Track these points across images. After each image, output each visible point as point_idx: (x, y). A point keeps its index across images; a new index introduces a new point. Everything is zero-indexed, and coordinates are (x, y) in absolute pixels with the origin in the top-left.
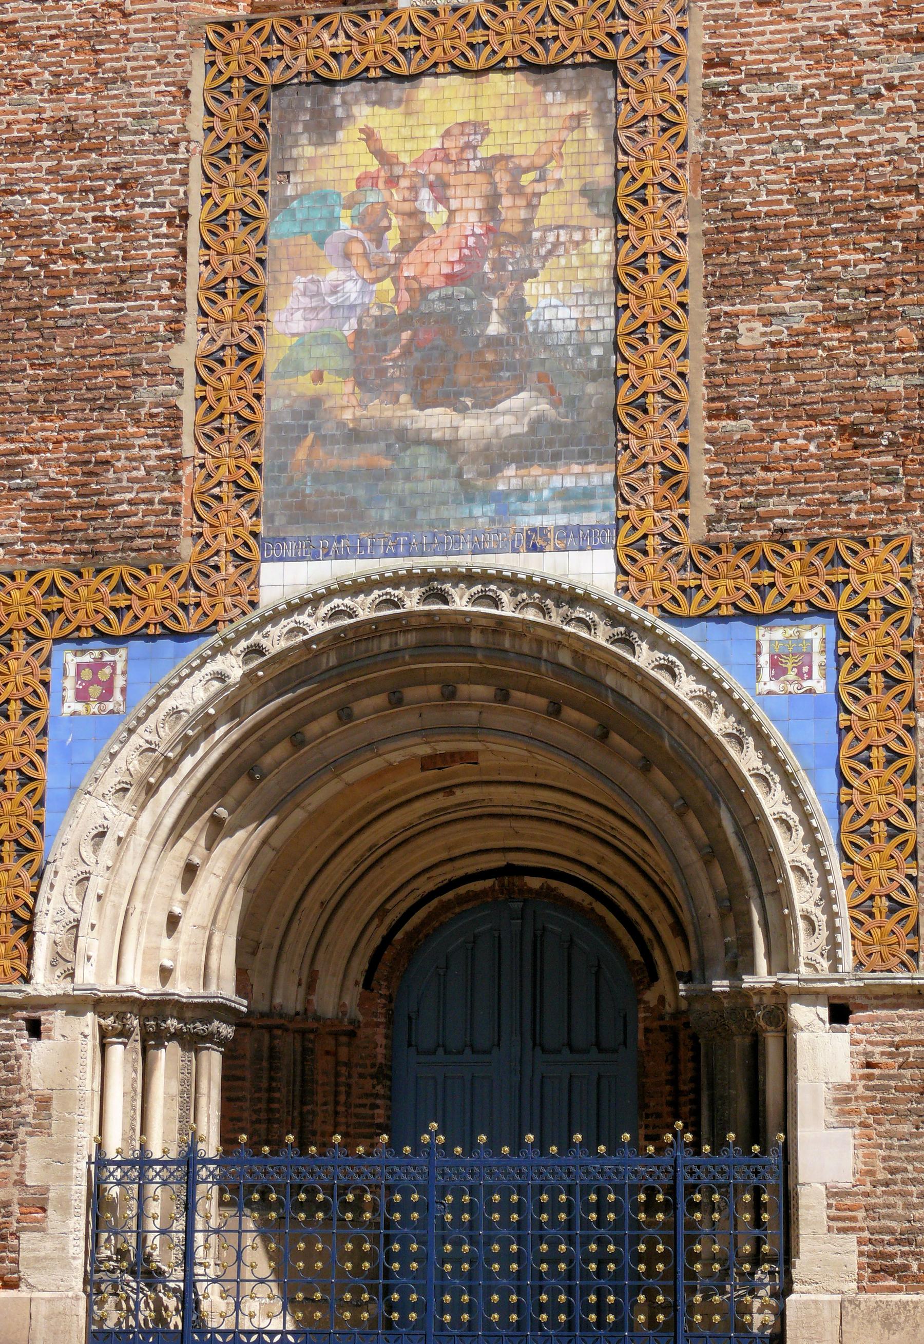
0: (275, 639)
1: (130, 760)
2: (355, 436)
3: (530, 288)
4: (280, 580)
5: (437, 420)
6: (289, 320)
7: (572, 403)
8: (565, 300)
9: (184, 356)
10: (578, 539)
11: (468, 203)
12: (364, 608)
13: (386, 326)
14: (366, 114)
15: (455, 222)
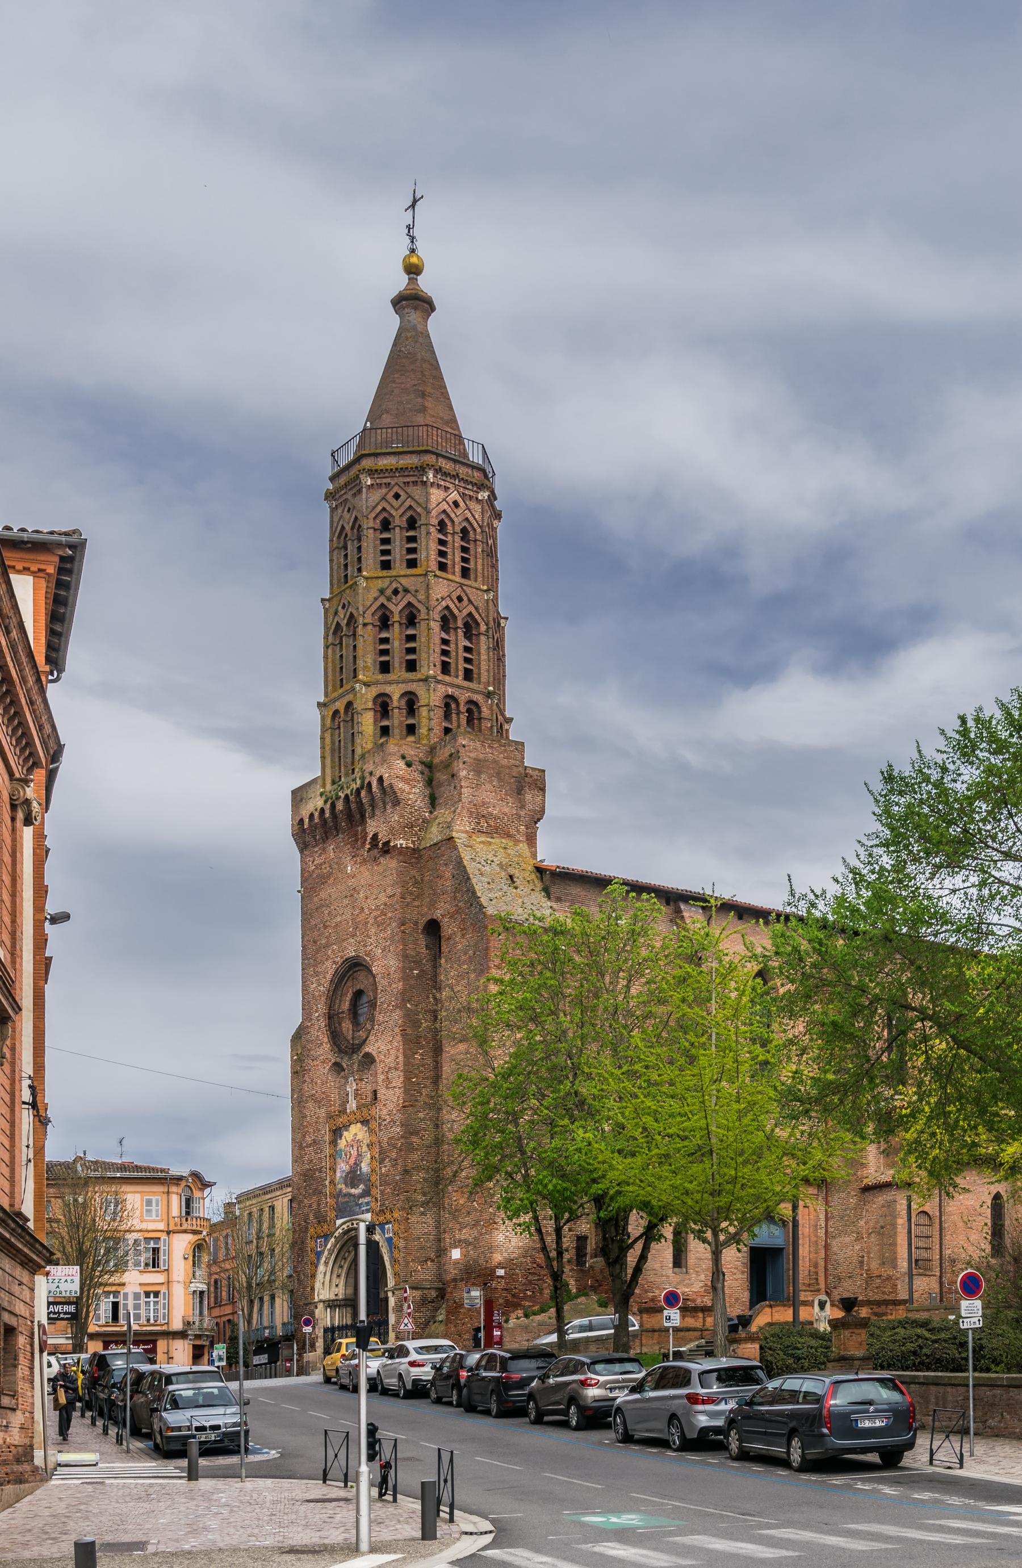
0: (337, 1234)
1: (323, 1259)
2: (345, 1195)
3: (363, 1165)
4: (339, 1222)
5: (353, 1191)
6: (338, 1175)
7: (366, 1186)
8: (365, 1167)
9: (327, 1183)
10: (368, 1211)
11: (355, 1149)
12: (345, 1226)
13: (348, 1173)
14: (345, 1133)
15: (354, 1152)
